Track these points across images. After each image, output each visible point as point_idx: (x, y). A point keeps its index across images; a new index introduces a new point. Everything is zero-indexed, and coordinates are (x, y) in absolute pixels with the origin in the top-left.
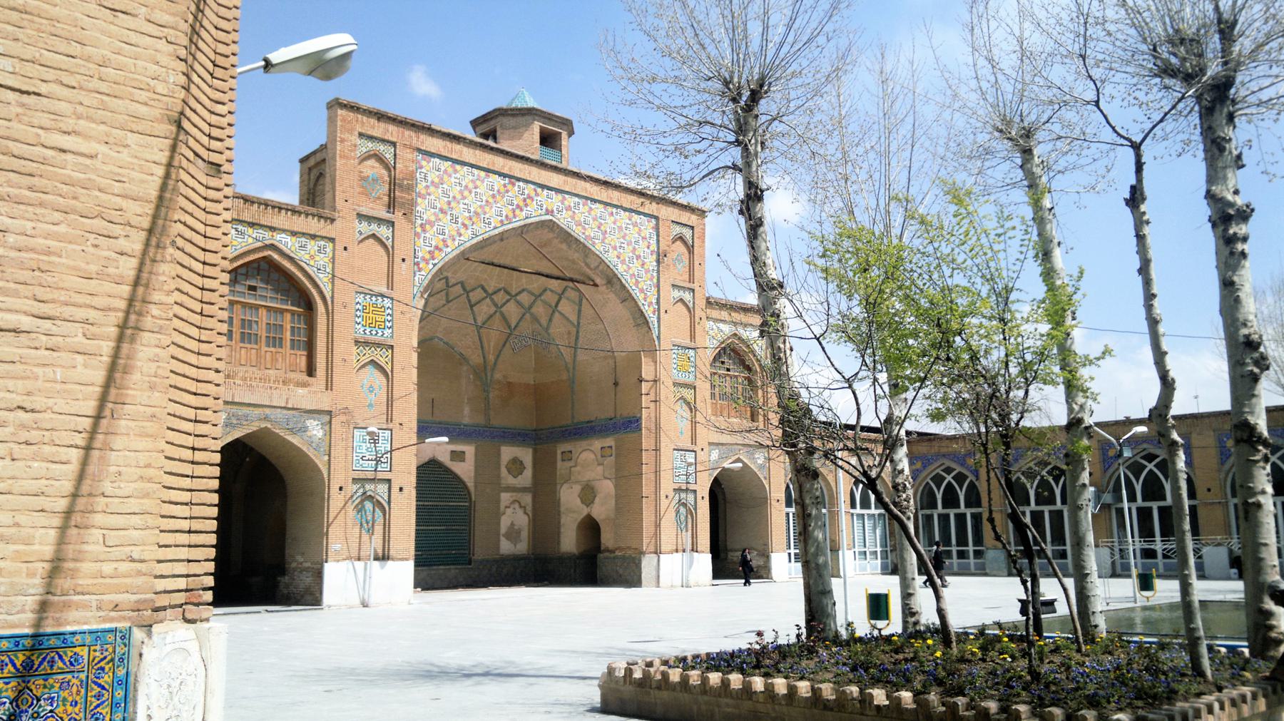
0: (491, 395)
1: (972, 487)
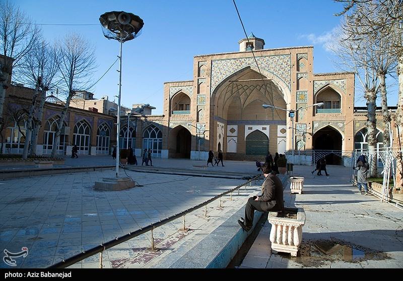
1: (135, 132)
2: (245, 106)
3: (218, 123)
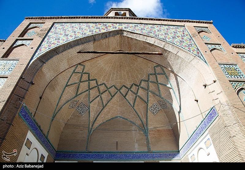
0: (149, 137)
2: (96, 125)
3: (30, 136)
